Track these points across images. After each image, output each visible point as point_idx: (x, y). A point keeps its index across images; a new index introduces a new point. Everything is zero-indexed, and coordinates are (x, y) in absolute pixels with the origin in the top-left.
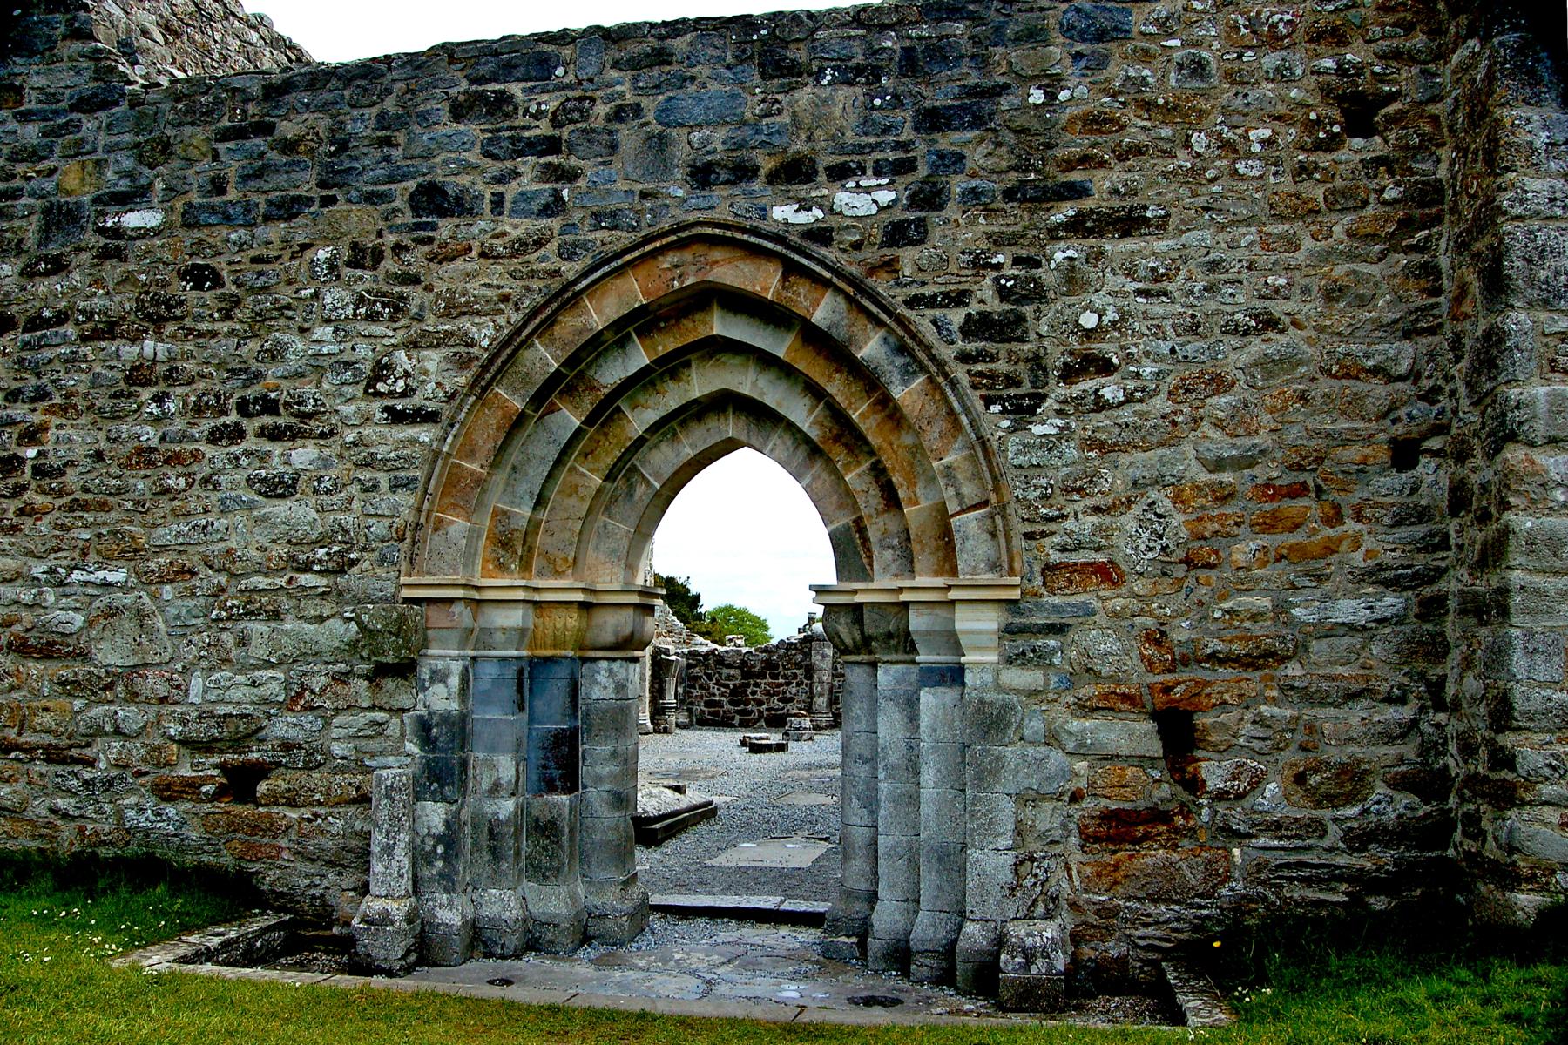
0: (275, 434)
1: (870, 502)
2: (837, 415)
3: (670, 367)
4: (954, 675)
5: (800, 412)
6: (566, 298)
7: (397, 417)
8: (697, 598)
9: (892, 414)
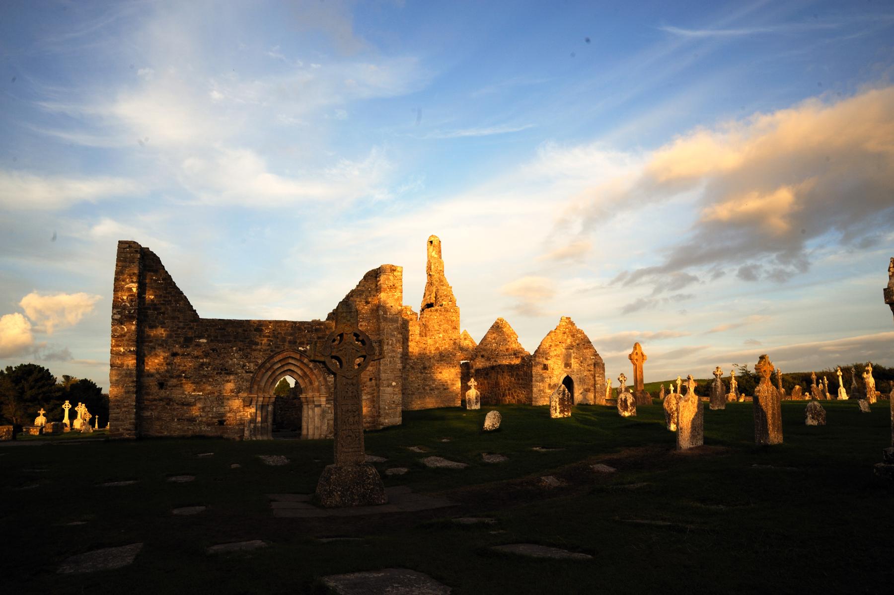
0: (227, 374)
1: (308, 384)
2: (305, 373)
3: (282, 366)
4: (320, 406)
5: (299, 372)
6: (272, 357)
7: (247, 372)
8: (100, 389)
9: (314, 374)
